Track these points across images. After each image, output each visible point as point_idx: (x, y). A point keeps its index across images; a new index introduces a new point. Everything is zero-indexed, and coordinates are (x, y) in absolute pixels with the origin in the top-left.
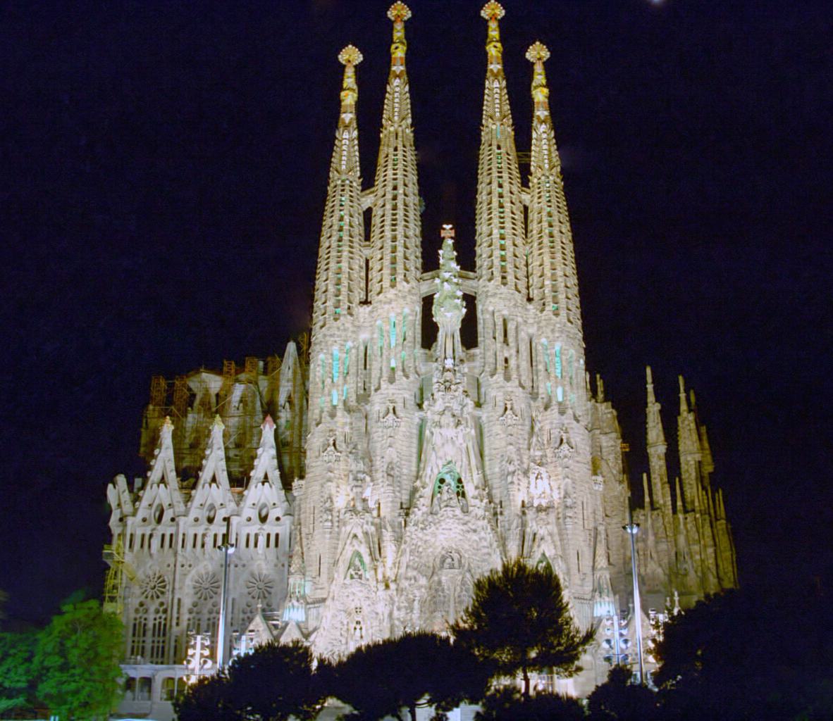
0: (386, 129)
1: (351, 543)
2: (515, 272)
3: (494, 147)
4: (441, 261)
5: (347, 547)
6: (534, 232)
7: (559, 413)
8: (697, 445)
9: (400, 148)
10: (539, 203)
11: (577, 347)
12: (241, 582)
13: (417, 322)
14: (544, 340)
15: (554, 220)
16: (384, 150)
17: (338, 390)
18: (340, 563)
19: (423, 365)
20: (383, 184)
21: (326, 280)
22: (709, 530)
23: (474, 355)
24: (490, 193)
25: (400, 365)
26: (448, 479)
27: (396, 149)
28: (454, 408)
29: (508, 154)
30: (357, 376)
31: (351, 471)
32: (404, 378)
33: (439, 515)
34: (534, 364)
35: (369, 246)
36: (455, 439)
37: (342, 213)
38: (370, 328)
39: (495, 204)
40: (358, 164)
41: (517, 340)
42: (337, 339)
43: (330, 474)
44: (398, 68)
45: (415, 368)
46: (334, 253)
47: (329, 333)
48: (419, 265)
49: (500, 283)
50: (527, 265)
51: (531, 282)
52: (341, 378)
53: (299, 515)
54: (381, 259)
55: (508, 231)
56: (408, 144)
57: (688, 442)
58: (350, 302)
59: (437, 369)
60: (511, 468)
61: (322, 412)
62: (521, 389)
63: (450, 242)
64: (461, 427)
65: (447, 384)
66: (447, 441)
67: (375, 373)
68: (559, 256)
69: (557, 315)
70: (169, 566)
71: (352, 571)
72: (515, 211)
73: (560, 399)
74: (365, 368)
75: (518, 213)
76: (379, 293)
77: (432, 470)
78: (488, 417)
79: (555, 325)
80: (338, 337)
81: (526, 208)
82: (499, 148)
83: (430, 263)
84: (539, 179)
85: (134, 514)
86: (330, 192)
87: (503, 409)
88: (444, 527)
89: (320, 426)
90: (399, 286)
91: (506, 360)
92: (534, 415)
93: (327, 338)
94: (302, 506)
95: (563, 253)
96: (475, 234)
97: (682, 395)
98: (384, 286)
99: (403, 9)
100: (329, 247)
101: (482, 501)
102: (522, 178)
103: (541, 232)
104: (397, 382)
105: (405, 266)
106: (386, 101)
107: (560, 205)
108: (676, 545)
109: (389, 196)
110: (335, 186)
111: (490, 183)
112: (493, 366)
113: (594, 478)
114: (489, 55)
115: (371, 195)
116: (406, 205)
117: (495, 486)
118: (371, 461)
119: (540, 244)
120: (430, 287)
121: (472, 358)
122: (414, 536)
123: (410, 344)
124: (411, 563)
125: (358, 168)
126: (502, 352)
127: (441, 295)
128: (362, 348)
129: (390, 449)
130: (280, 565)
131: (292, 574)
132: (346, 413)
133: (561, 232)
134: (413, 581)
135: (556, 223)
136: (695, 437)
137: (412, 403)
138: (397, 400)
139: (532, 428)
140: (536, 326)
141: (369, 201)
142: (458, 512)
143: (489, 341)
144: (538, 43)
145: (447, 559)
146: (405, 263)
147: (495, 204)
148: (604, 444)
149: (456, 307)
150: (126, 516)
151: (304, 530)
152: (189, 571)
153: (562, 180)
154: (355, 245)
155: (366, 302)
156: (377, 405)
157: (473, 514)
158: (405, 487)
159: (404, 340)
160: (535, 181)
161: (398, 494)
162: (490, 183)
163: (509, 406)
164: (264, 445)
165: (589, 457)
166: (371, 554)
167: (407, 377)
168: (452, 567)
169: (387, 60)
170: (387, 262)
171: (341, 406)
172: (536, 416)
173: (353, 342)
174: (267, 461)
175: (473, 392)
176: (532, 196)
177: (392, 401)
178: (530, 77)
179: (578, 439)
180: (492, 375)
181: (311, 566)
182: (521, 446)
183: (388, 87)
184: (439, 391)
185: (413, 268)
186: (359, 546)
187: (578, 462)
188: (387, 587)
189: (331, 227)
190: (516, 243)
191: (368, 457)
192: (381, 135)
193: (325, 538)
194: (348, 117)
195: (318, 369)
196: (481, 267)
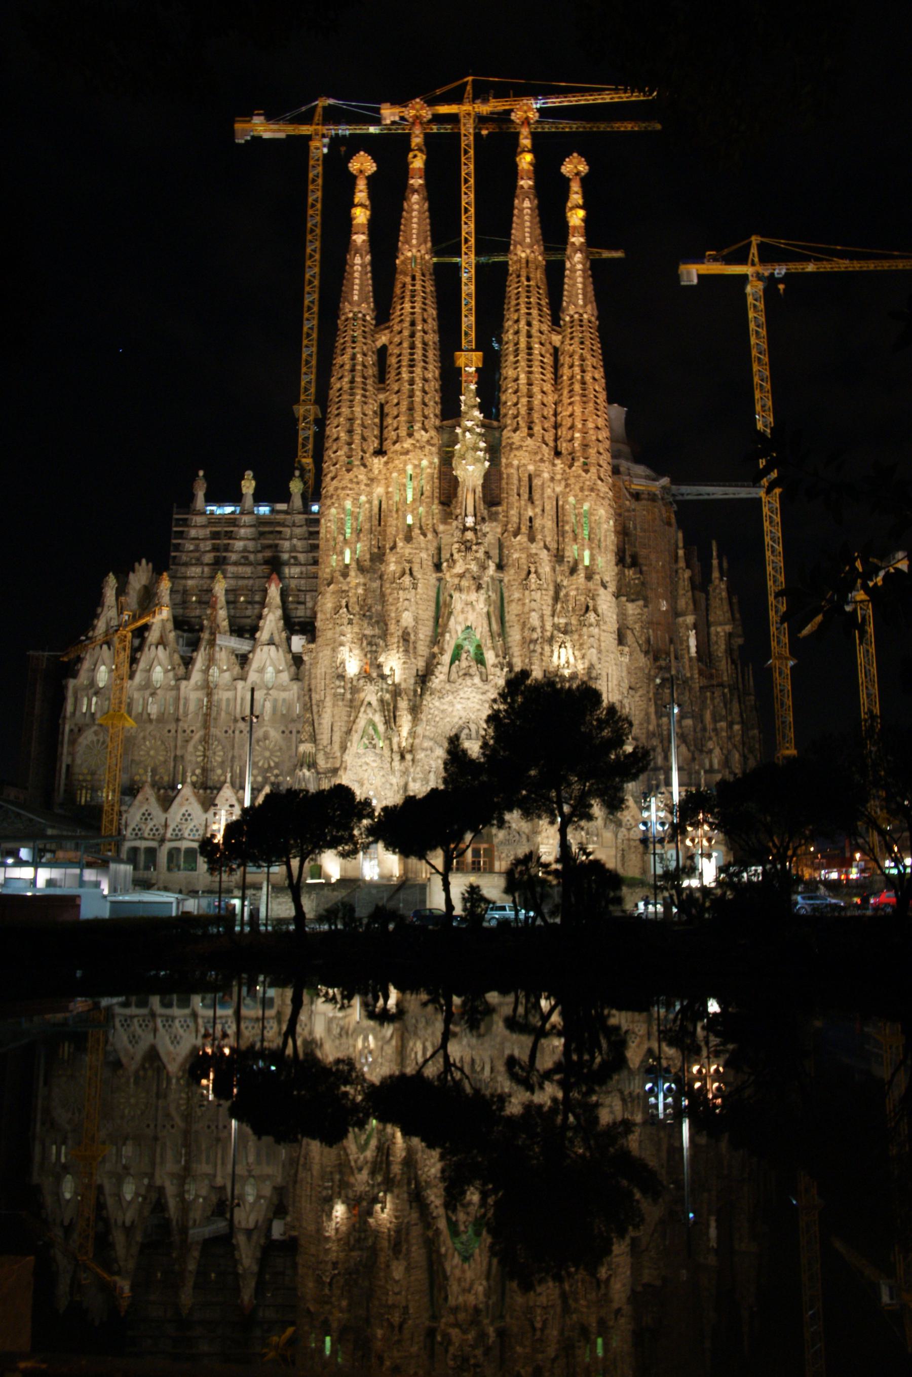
1: (365, 711)
2: (542, 422)
3: (523, 279)
4: (463, 408)
5: (361, 715)
6: (565, 378)
8: (728, 615)
9: (418, 275)
10: (571, 345)
11: (607, 507)
14: (572, 499)
15: (587, 365)
18: (353, 732)
20: (399, 319)
22: (737, 706)
23: (497, 513)
24: (517, 332)
25: (418, 522)
27: (414, 278)
29: (539, 288)
30: (371, 533)
32: (422, 537)
34: (560, 524)
35: (384, 389)
36: (474, 603)
39: (523, 345)
40: (371, 294)
41: (542, 497)
42: (349, 492)
43: (342, 638)
44: (417, 182)
46: (345, 397)
47: (341, 485)
48: (438, 412)
50: (555, 414)
51: (559, 433)
52: (354, 536)
54: (398, 404)
56: (427, 273)
57: (719, 612)
58: (364, 452)
59: (457, 527)
60: (535, 636)
62: (545, 552)
63: (473, 387)
64: (482, 591)
67: (391, 531)
69: (587, 471)
70: (169, 731)
71: (365, 740)
72: (543, 353)
74: (380, 525)
75: (548, 355)
76: (395, 443)
78: (509, 581)
80: (351, 489)
81: (556, 349)
82: (528, 279)
85: (131, 676)
87: (525, 572)
88: (462, 695)
89: (332, 586)
90: (417, 435)
91: (531, 519)
92: (559, 580)
93: (339, 491)
95: (596, 403)
97: (715, 562)
99: (422, 109)
100: (340, 389)
101: (502, 669)
102: (552, 316)
103: (572, 378)
104: (414, 541)
105: (423, 413)
106: (403, 221)
107: (594, 348)
108: (702, 722)
109: (406, 333)
110: (347, 320)
113: (620, 648)
114: (520, 168)
115: (386, 331)
116: (425, 344)
118: (386, 625)
119: (571, 391)
122: (430, 705)
123: (428, 500)
124: (427, 733)
125: (372, 300)
128: (376, 503)
130: (287, 732)
132: (359, 573)
133: (594, 379)
134: (429, 752)
135: (590, 368)
136: (726, 607)
137: (430, 563)
140: (563, 483)
142: (477, 680)
144: (575, 155)
146: (423, 409)
147: (523, 345)
148: (631, 612)
151: (315, 697)
152: (191, 738)
153: (598, 318)
154: (369, 387)
155: (380, 452)
156: (392, 567)
157: (493, 683)
158: (421, 653)
159: (422, 494)
160: (568, 319)
163: (533, 570)
164: (269, 606)
165: (616, 626)
167: (425, 535)
169: (404, 171)
170: (404, 407)
171: (354, 565)
172: (562, 581)
174: (273, 624)
175: (495, 553)
176: (563, 337)
177: (410, 562)
178: (566, 197)
179: (605, 607)
180: (515, 535)
183: (405, 205)
185: (432, 416)
186: (373, 714)
187: (604, 631)
188: (403, 757)
190: (545, 389)
191: (381, 621)
192: (398, 262)
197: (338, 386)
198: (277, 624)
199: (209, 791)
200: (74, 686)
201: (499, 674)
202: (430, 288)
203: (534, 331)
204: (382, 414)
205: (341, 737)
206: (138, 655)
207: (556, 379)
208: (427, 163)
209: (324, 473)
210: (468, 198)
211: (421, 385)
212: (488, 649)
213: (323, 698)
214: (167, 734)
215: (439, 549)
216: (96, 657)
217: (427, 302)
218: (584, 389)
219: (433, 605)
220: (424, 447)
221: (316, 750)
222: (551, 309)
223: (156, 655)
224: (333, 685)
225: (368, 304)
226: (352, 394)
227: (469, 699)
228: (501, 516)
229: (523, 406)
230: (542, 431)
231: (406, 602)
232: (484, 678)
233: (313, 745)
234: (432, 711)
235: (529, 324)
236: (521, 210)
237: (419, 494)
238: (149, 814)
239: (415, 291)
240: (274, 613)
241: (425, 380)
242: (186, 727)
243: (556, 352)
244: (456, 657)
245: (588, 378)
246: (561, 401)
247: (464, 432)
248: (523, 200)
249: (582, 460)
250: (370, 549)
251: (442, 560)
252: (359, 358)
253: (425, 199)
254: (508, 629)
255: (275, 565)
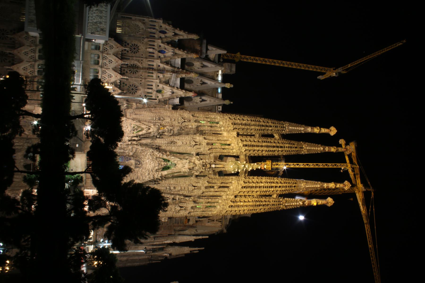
0: (304, 144)
1: (147, 127)
2: (247, 191)
3: (294, 185)
4: (252, 164)
5: (145, 126)
6: (261, 199)
7: (192, 207)
9: (297, 149)
10: (272, 201)
12: (135, 82)
13: (229, 154)
15: (265, 207)
16: (296, 143)
17: (205, 123)
18: (139, 123)
19: (213, 156)
20: (283, 142)
21: (247, 120)
24: (277, 183)
26: (169, 164)
27: (296, 148)
28: (196, 168)
29: (292, 190)
30: (210, 131)
31: (174, 128)
32: (208, 149)
33: (156, 161)
34: (211, 197)
35: (260, 136)
36: (185, 167)
37: (273, 127)
38: (228, 136)
39: (273, 185)
44: (327, 149)
45: (212, 153)
46: (257, 123)
47: (227, 121)
49: (242, 186)
50: (249, 196)
51: (243, 197)
52: (210, 125)
53: (158, 107)
54: (254, 141)
55: (262, 189)
58: (238, 129)
59: (211, 162)
60: (172, 188)
61: (197, 117)
62: (202, 192)
63: (259, 168)
64: (189, 171)
65: (205, 165)
66: (184, 165)
67: (211, 138)
68: (252, 208)
69: (229, 207)
70: (142, 55)
72: (270, 192)
73: (197, 207)
74: (213, 134)
75: (269, 193)
76: (241, 140)
77: (173, 159)
78: (192, 179)
79: (225, 206)
80: (226, 124)
81: (271, 196)
82: (294, 187)
83: (253, 159)
84: (282, 201)
86: (281, 122)
87: (195, 185)
88: (151, 162)
89: (192, 116)
90: (243, 148)
91: (213, 187)
92: (192, 197)
93: (225, 120)
94: (162, 108)
95: (253, 210)
96: (262, 176)
97: (197, 249)
98: (244, 142)
100: (260, 122)
103: (261, 201)
105: (251, 150)
106: (314, 144)
107: (271, 209)
109: (278, 145)
110: (283, 124)
111: (281, 183)
112: (211, 182)
113: (167, 218)
115: (279, 138)
116: (274, 151)
117: (166, 181)
118: (178, 135)
119: (257, 201)
120: (242, 159)
121: (215, 174)
124: (138, 150)
125: (289, 133)
126: (216, 186)
127: (239, 164)
128: (221, 133)
129: (182, 143)
131: (136, 104)
133: (261, 209)
134: (131, 150)
135: (264, 207)
137: (199, 151)
138: (200, 146)
139: (187, 196)
140: (226, 198)
141: (277, 137)
142: (157, 168)
143: (221, 181)
144: (334, 202)
145: (139, 163)
146: (252, 150)
147: (273, 185)
149: (234, 170)
150: (162, 40)
151: (153, 109)
152: (140, 63)
153: (281, 210)
154: (260, 131)
155: (238, 135)
156: (199, 138)
158: (167, 148)
159: (223, 149)
160: (281, 200)
161: (165, 145)
162: (281, 183)
163: (196, 188)
164: (186, 92)
166: (142, 135)
167: (209, 150)
168: (136, 164)
171: (199, 124)
172: (191, 198)
173: (223, 130)
175: (202, 174)
179: (182, 213)
180: (208, 182)
181: (139, 111)
182: (180, 192)
184: (203, 162)
185: (250, 153)
187: (173, 213)
188: (129, 141)
189: (268, 122)
190: (258, 192)
191: (179, 134)
192: (302, 142)
193: (149, 117)
194: (309, 130)
195: (214, 116)
196: (249, 178)
197: (261, 121)
198: (179, 95)
199: (120, 70)
200: (160, 22)
201: (159, 176)
202: (293, 153)
203: (277, 189)
204: (251, 135)
205: (138, 118)
206: (170, 45)
207: (261, 196)
208: (333, 152)
209: (232, 115)
210: (321, 165)
211: (260, 149)
212: (168, 172)
213: (152, 112)
214: (141, 54)
215: (204, 154)
216: (170, 30)
217: (288, 152)
218: (257, 206)
219: (184, 152)
220: (240, 150)
221: (133, 109)
222: (284, 194)
223: (170, 52)
224: (156, 116)
225: (288, 132)
226: (258, 126)
227: (150, 165)
228: (215, 176)
229: (252, 185)
230: (244, 191)
231: (185, 143)
232: (157, 170)
233: (135, 108)
234: (146, 151)
235: (280, 187)
236: (317, 184)
237: (223, 148)
238: (112, 48)
239: (292, 148)
240: (183, 94)
241: (262, 151)
242: (143, 61)
243: (270, 196)
244: (165, 160)
245: (261, 207)
246: (254, 198)
247: (244, 164)
248: (320, 185)
249: (233, 205)
250: (204, 130)
251: (200, 156)
252: (270, 128)
253: (321, 152)
254: (175, 179)
255: (200, 94)
